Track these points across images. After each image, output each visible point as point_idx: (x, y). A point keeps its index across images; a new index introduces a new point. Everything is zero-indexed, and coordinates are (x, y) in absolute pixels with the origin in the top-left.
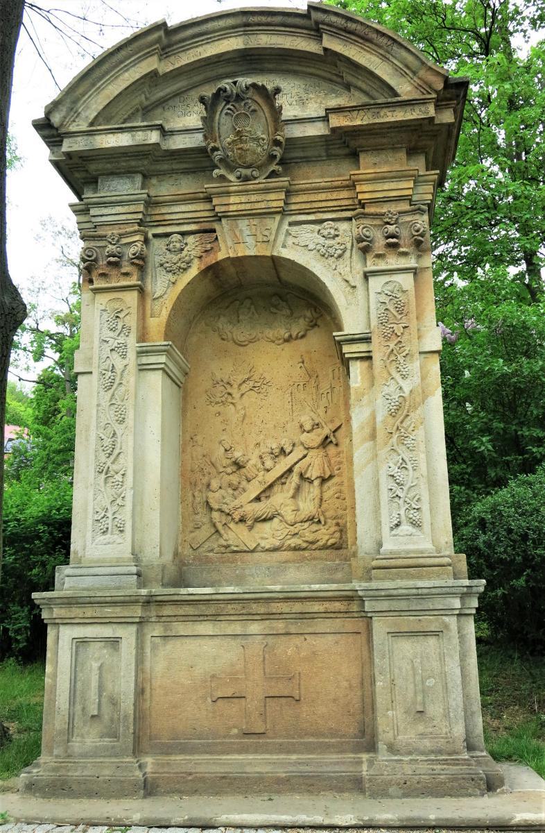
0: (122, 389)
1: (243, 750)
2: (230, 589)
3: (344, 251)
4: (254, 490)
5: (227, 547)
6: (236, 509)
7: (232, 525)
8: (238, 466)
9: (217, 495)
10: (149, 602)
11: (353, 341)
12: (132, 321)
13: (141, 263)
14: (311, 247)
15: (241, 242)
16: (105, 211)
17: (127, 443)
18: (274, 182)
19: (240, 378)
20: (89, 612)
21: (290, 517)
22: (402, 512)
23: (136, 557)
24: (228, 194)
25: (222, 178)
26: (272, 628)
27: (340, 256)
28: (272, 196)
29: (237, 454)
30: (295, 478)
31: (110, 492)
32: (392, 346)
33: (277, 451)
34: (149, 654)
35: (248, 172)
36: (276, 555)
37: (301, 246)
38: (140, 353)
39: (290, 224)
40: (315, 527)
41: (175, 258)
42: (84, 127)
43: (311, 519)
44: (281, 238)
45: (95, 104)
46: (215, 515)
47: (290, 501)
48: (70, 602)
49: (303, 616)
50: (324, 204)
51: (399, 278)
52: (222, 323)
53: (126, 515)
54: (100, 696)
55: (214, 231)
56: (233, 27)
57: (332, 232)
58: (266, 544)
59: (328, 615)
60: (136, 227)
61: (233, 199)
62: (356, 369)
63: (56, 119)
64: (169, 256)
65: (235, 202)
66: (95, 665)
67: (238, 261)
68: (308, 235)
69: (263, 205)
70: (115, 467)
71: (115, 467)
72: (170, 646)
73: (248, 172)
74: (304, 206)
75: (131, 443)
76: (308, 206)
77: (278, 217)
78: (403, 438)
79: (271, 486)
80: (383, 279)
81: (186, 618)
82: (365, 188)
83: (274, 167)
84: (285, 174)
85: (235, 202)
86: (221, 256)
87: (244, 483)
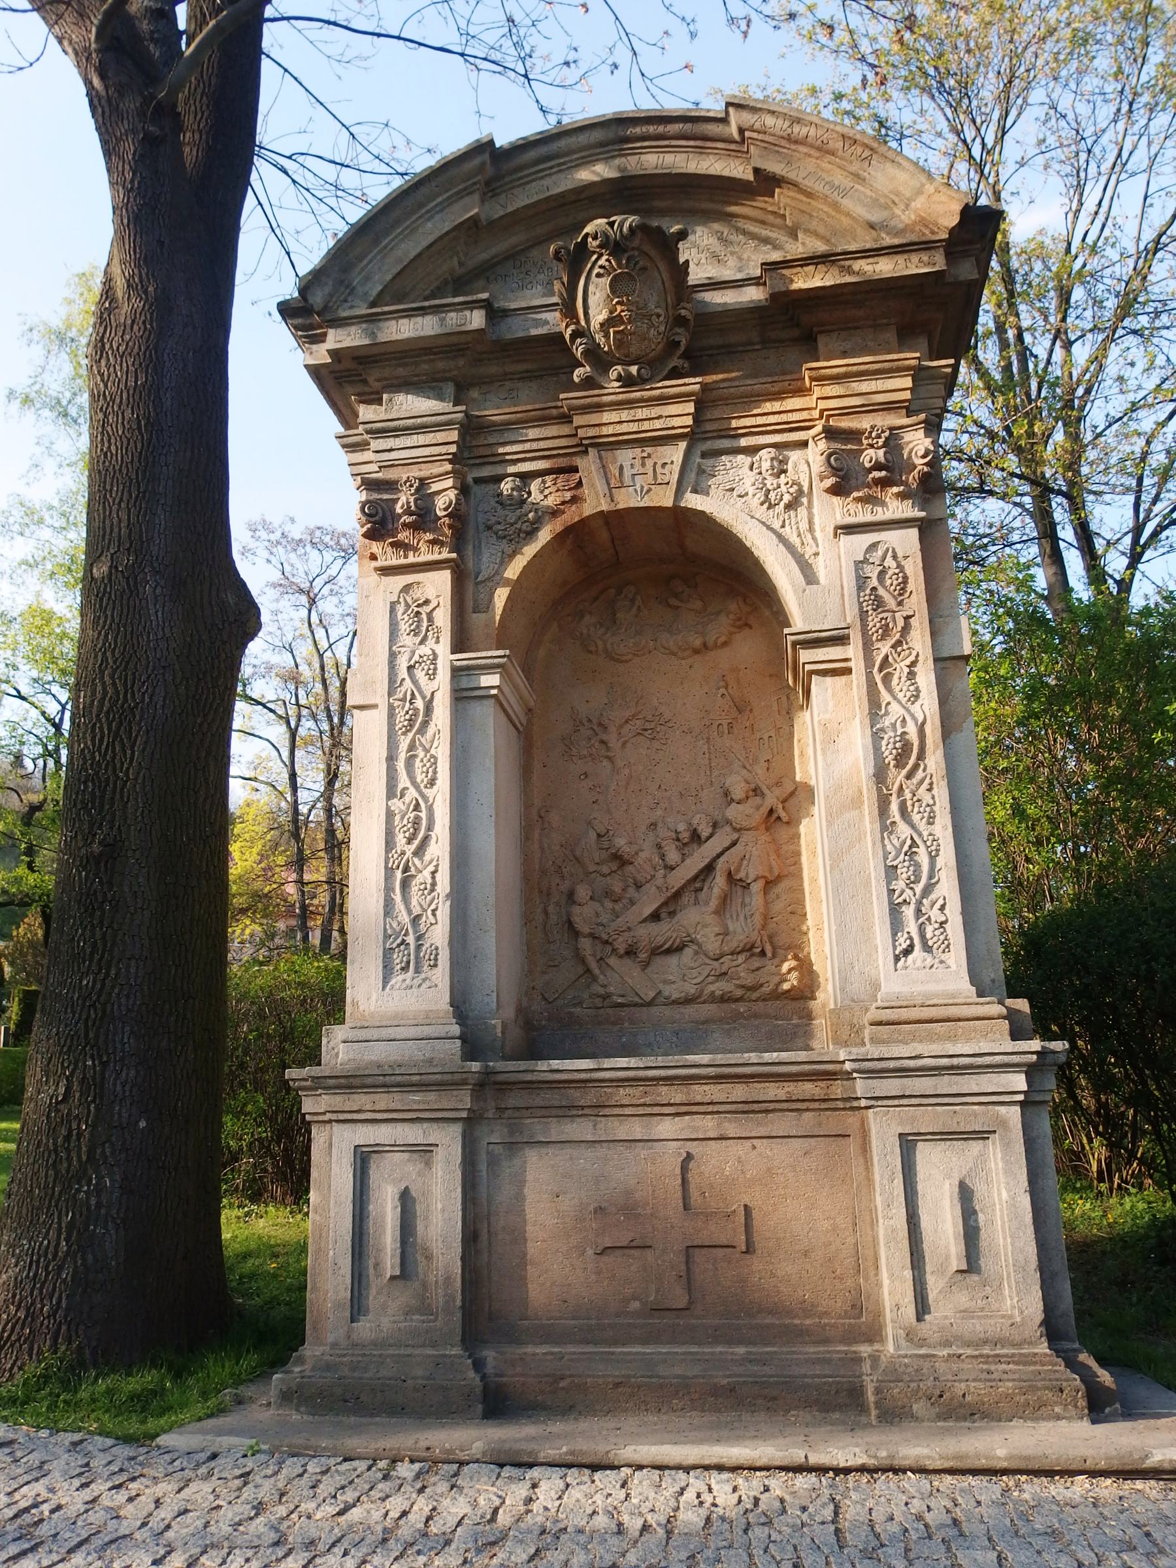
5: (607, 996)
7: (612, 961)
8: (621, 860)
21: (712, 945)
23: (460, 1005)
24: (599, 408)
26: (695, 1129)
30: (719, 881)
33: (685, 836)
34: (484, 1173)
39: (704, 455)
40: (756, 962)
43: (748, 949)
45: (379, 272)
47: (710, 919)
48: (350, 1082)
55: (575, 470)
56: (602, 144)
61: (607, 417)
63: (317, 298)
64: (501, 512)
65: (613, 423)
67: (615, 520)
79: (677, 895)
83: (675, 362)
86: (588, 509)
87: (631, 891)
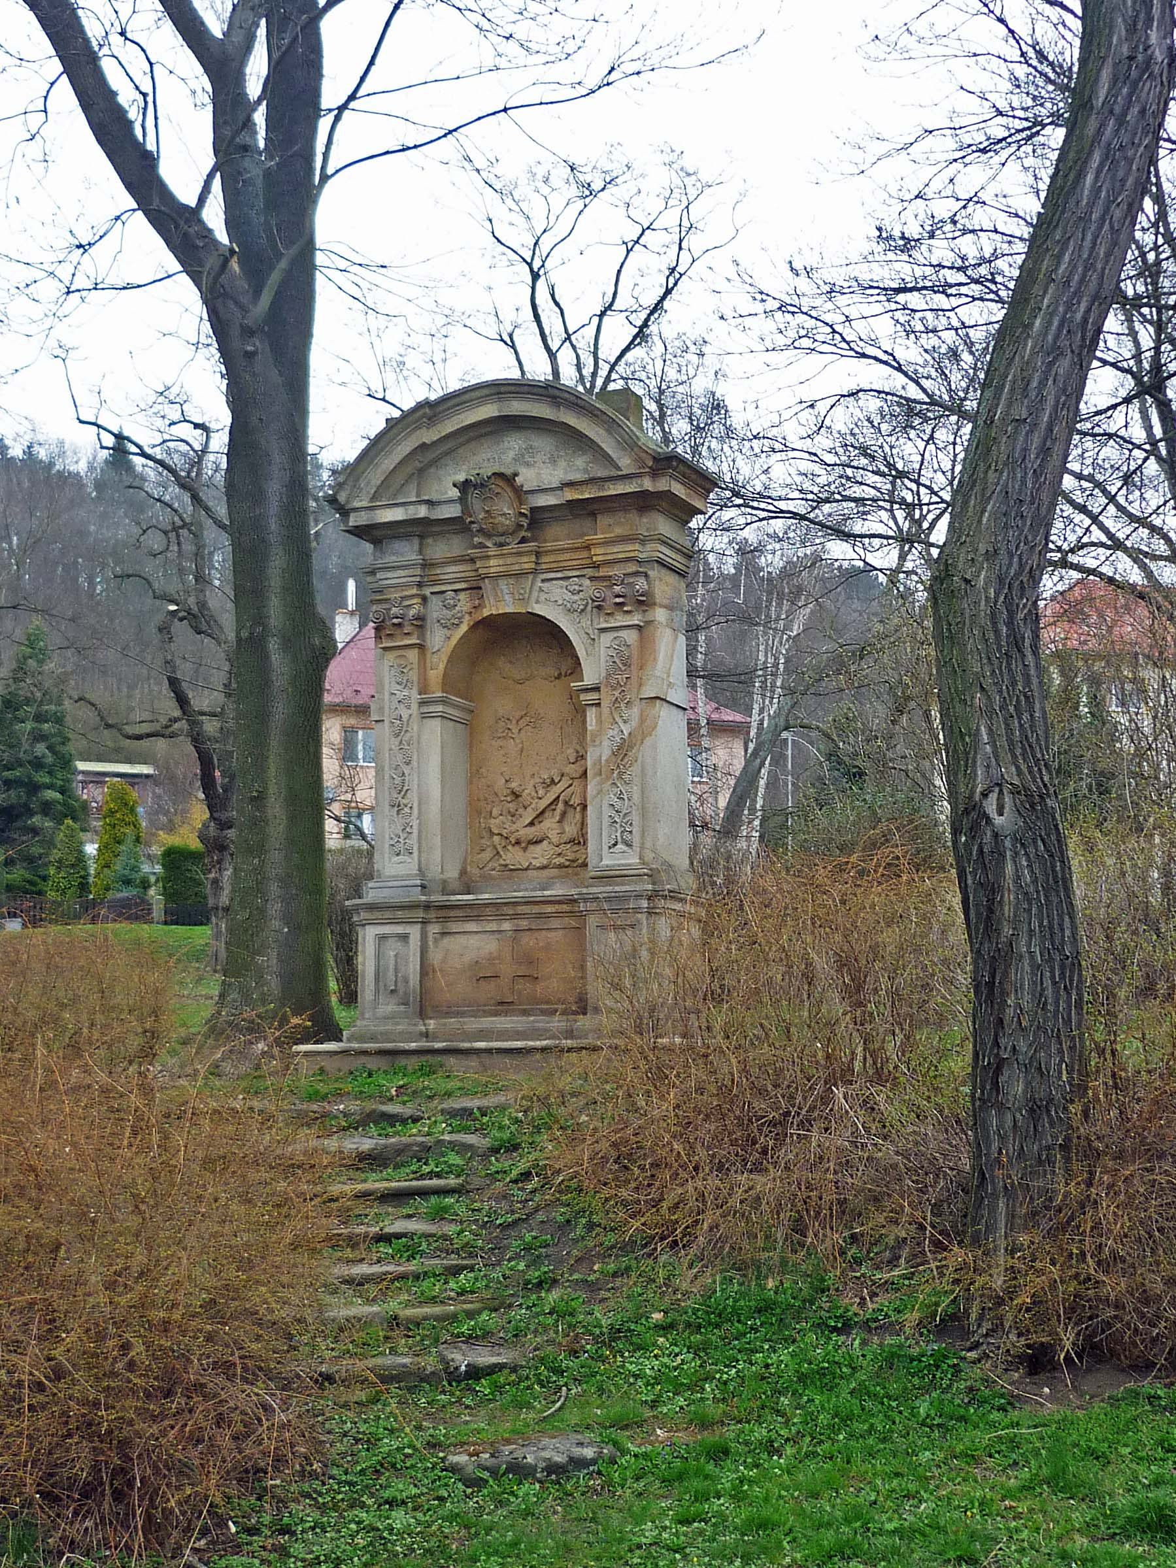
0: (408, 735)
1: (496, 1014)
2: (487, 896)
3: (586, 605)
4: (528, 817)
5: (506, 865)
6: (512, 833)
7: (510, 847)
8: (516, 795)
9: (497, 821)
10: (427, 906)
11: (587, 690)
12: (414, 676)
13: (420, 622)
14: (560, 602)
15: (503, 602)
16: (389, 575)
17: (413, 783)
18: (525, 547)
19: (518, 714)
20: (388, 914)
21: (555, 840)
22: (618, 834)
23: (421, 872)
24: (488, 557)
25: (482, 546)
26: (518, 925)
27: (582, 610)
28: (525, 559)
29: (514, 785)
30: (561, 806)
31: (399, 822)
32: (617, 693)
33: (548, 781)
35: (502, 539)
36: (546, 872)
37: (551, 602)
38: (422, 703)
39: (543, 581)
40: (576, 848)
41: (449, 614)
42: (365, 504)
43: (572, 841)
44: (535, 594)
45: (375, 476)
46: (496, 839)
47: (555, 826)
48: (372, 907)
49: (540, 916)
50: (569, 563)
51: (623, 634)
52: (501, 662)
53: (413, 841)
54: (396, 976)
55: (480, 588)
56: (487, 396)
57: (577, 588)
58: (537, 863)
59: (559, 914)
60: (414, 591)
61: (492, 562)
62: (591, 715)
64: (445, 611)
65: (494, 565)
66: (392, 953)
68: (558, 591)
69: (516, 567)
70: (405, 801)
71: (405, 801)
72: (446, 940)
73: (502, 539)
74: (552, 565)
75: (416, 782)
76: (555, 565)
77: (531, 577)
78: (620, 774)
79: (542, 813)
80: (610, 636)
81: (458, 919)
82: (599, 551)
83: (523, 533)
84: (534, 539)
85: (494, 565)
87: (521, 810)
